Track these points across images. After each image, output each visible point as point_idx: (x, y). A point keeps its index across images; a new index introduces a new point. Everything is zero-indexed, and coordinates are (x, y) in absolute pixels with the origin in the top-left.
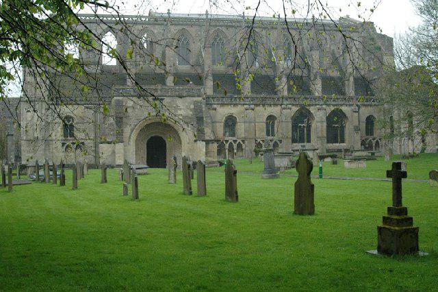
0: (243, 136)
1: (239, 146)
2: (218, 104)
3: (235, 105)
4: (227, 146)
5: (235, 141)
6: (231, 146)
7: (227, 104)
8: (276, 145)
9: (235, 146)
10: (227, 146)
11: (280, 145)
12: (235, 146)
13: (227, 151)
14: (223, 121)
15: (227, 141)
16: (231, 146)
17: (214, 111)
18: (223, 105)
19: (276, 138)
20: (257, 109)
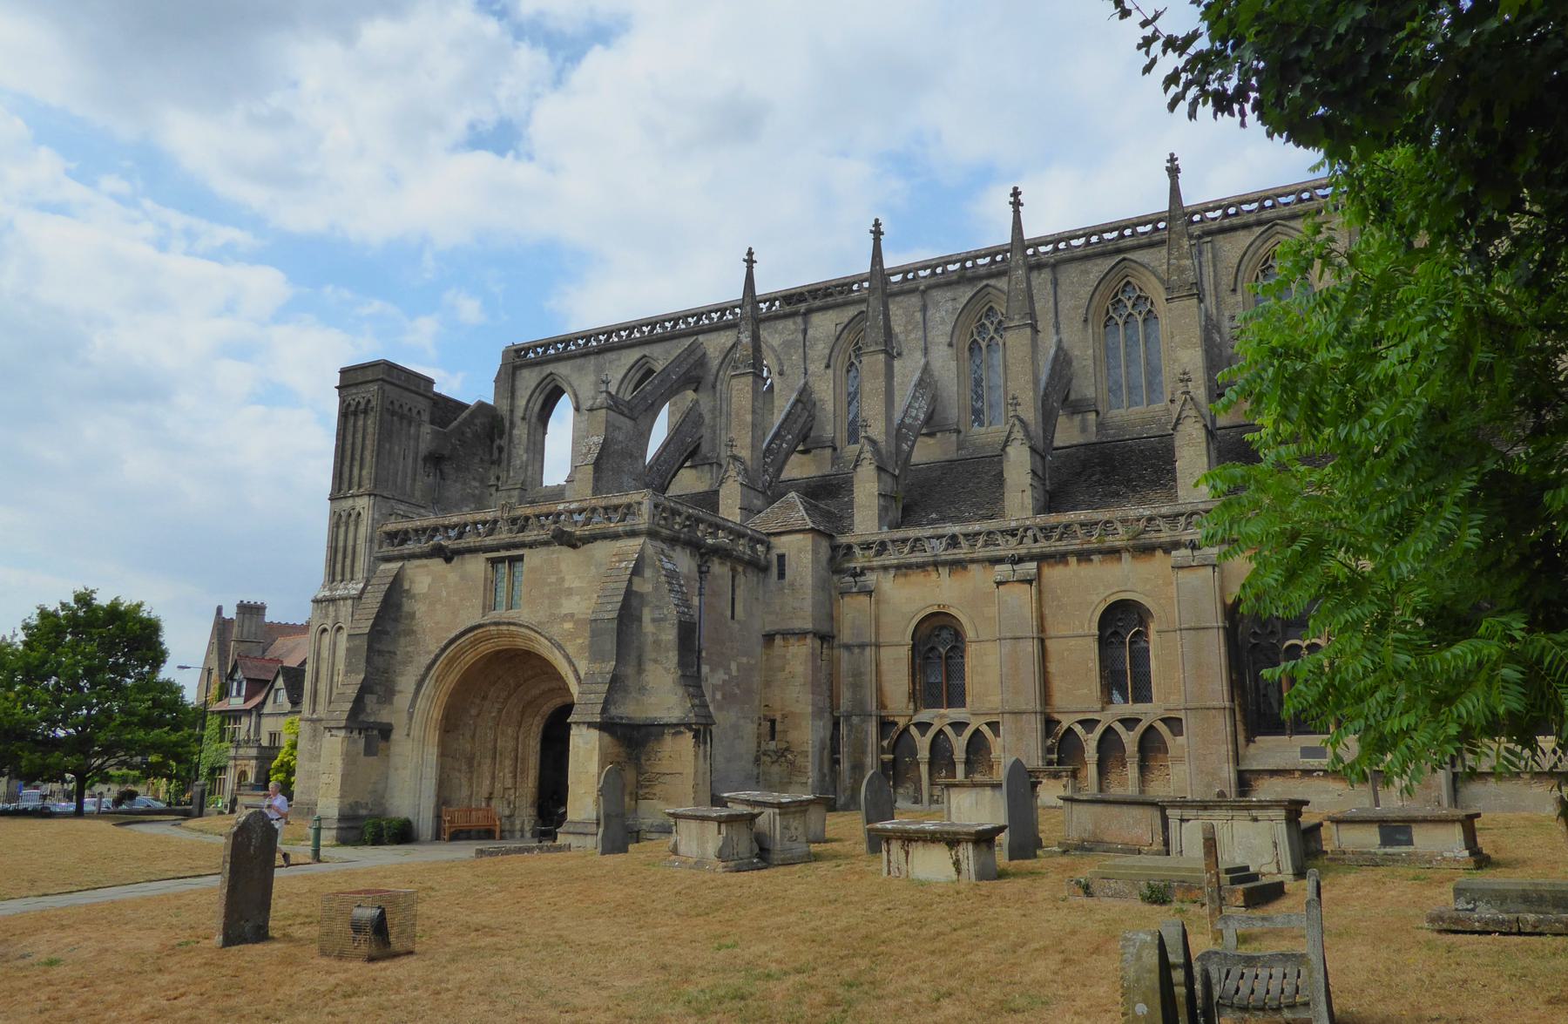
0: (994, 701)
1: (977, 745)
2: (885, 568)
3: (957, 565)
4: (923, 744)
5: (959, 726)
6: (939, 748)
7: (922, 566)
8: (1151, 745)
9: (959, 744)
10: (923, 744)
11: (1175, 743)
12: (959, 744)
13: (924, 769)
14: (908, 639)
15: (923, 727)
16: (939, 748)
17: (864, 599)
18: (903, 569)
19: (1149, 713)
20: (1053, 574)
